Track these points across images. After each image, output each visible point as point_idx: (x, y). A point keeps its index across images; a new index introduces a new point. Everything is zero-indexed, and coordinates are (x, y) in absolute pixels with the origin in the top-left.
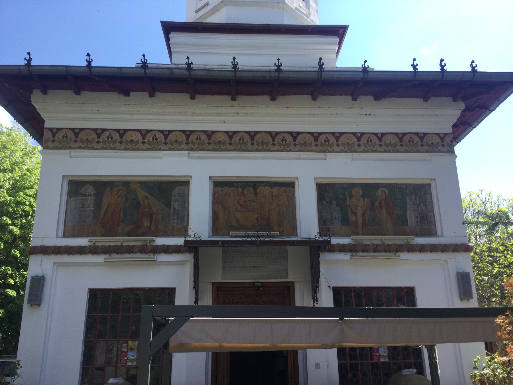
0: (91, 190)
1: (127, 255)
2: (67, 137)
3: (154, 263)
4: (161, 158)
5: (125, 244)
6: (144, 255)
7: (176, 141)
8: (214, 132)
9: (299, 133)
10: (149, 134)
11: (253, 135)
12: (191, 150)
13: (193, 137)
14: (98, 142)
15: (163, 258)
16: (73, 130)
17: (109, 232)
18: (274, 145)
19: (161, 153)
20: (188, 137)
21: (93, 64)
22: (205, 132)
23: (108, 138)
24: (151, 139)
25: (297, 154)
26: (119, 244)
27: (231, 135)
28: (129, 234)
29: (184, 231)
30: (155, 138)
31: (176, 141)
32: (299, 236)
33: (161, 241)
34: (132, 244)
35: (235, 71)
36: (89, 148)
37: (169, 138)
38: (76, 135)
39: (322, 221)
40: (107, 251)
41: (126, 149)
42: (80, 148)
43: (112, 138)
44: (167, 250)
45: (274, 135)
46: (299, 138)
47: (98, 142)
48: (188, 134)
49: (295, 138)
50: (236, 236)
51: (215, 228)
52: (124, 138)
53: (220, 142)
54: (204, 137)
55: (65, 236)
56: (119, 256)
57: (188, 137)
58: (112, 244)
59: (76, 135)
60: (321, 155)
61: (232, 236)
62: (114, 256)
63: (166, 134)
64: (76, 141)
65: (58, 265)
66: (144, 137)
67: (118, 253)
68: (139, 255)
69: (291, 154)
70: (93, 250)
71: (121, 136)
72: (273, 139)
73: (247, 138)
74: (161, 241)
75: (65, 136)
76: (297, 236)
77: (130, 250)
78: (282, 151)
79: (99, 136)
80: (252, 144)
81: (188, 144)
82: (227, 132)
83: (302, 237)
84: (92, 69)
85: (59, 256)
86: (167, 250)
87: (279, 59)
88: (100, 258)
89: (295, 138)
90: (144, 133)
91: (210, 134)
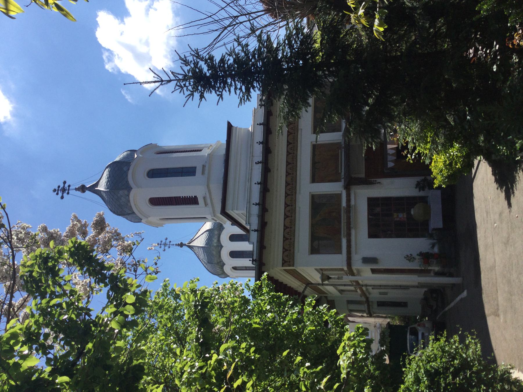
0: (316, 243)
1: (352, 220)
2: (287, 255)
3: (355, 205)
4: (300, 208)
5: (345, 221)
6: (352, 212)
7: (291, 201)
8: (286, 182)
9: (288, 142)
10: (287, 214)
11: (288, 163)
12: (296, 193)
13: (289, 192)
14: (291, 239)
15: (353, 203)
16: (283, 252)
17: (338, 232)
18: (294, 153)
19: (297, 208)
20: (288, 195)
21: (256, 229)
22: (286, 186)
23: (288, 234)
24: (289, 213)
25: (299, 142)
26: (345, 224)
27: (288, 174)
28: (340, 222)
29: (339, 196)
30: (289, 211)
31: (291, 201)
32: (341, 141)
33: (344, 204)
34: (345, 217)
35: (262, 163)
36: (294, 244)
37: (289, 204)
38: (286, 250)
39: (334, 131)
40: (349, 229)
41: (295, 225)
42: (294, 248)
43: (288, 232)
44: (348, 200)
45: (288, 153)
46: (291, 142)
47: (291, 239)
48: (287, 195)
49: (291, 143)
50: (342, 169)
51: (337, 180)
52: (288, 226)
53: (292, 179)
54: (289, 187)
55: (341, 253)
56: (352, 223)
57: (288, 195)
58: (345, 227)
59: (286, 250)
60: (299, 132)
61: (342, 171)
62: (352, 226)
63: (286, 205)
64: (290, 250)
65: (356, 253)
66: (288, 217)
67: (350, 224)
68: (351, 214)
69: (299, 145)
70: (349, 236)
71: (287, 228)
72: (290, 153)
73: (290, 166)
74: (344, 204)
75: (287, 256)
76: (341, 143)
77: (349, 218)
78: (297, 150)
79: (287, 239)
80: (293, 163)
81: (292, 195)
82: (286, 176)
83: (342, 138)
84: (259, 230)
85: (352, 252)
86: (348, 200)
87: (257, 143)
88: (353, 232)
89: (291, 143)
90: (286, 216)
91: (287, 184)
